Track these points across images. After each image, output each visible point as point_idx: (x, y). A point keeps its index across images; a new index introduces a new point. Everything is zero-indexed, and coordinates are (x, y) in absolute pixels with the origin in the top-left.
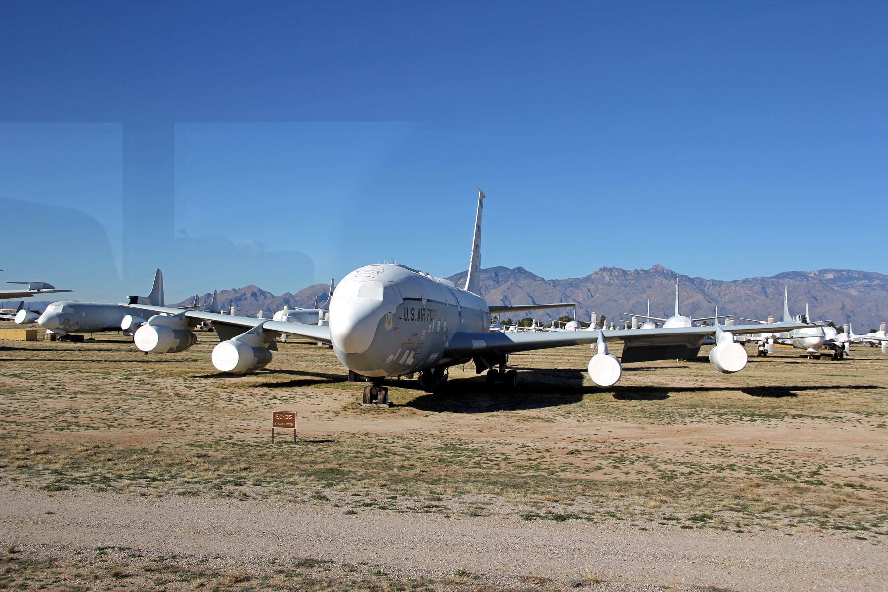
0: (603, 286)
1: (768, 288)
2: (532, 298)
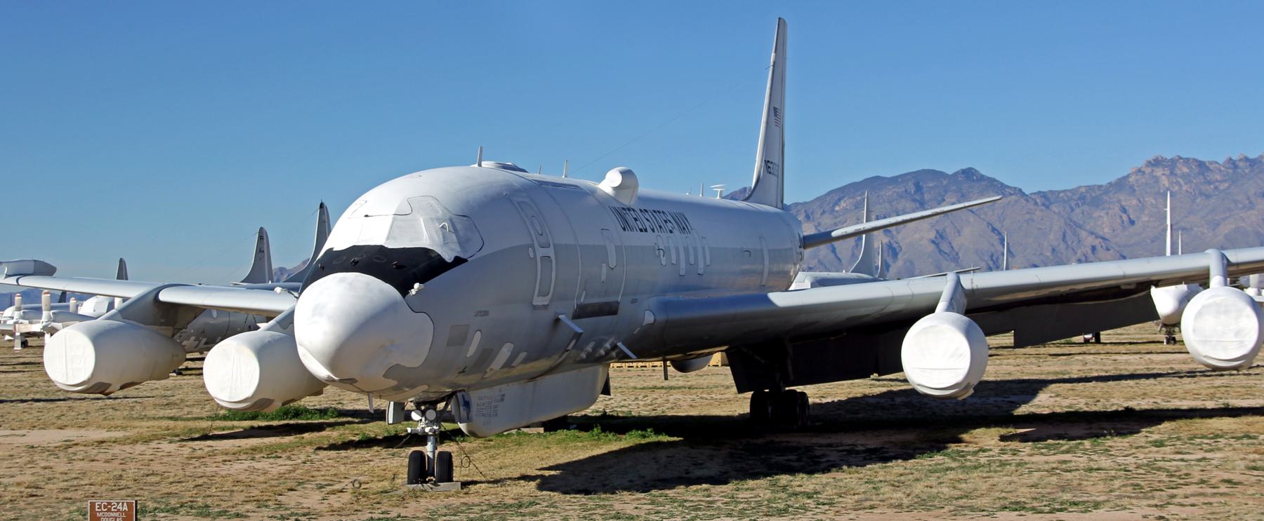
0: (1155, 200)
2: (999, 234)
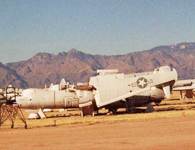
1: (135, 58)
